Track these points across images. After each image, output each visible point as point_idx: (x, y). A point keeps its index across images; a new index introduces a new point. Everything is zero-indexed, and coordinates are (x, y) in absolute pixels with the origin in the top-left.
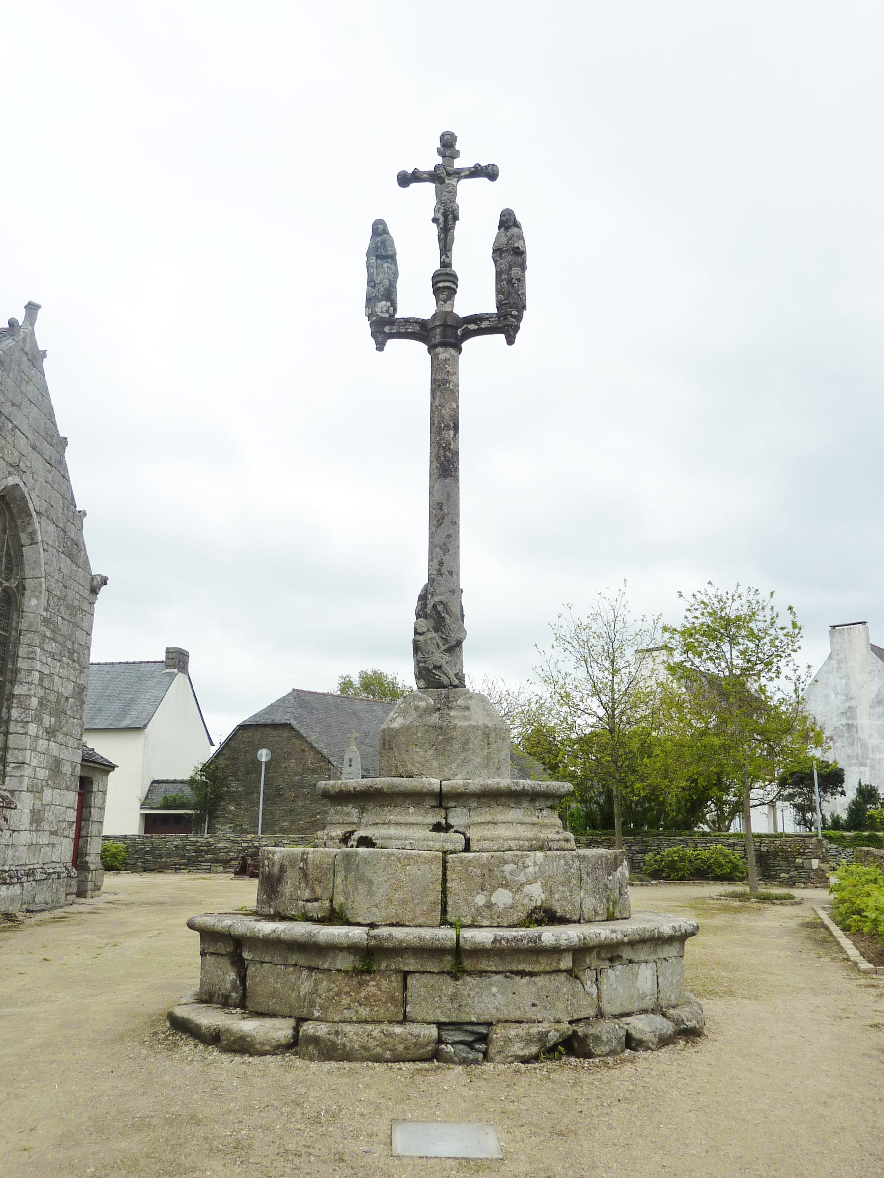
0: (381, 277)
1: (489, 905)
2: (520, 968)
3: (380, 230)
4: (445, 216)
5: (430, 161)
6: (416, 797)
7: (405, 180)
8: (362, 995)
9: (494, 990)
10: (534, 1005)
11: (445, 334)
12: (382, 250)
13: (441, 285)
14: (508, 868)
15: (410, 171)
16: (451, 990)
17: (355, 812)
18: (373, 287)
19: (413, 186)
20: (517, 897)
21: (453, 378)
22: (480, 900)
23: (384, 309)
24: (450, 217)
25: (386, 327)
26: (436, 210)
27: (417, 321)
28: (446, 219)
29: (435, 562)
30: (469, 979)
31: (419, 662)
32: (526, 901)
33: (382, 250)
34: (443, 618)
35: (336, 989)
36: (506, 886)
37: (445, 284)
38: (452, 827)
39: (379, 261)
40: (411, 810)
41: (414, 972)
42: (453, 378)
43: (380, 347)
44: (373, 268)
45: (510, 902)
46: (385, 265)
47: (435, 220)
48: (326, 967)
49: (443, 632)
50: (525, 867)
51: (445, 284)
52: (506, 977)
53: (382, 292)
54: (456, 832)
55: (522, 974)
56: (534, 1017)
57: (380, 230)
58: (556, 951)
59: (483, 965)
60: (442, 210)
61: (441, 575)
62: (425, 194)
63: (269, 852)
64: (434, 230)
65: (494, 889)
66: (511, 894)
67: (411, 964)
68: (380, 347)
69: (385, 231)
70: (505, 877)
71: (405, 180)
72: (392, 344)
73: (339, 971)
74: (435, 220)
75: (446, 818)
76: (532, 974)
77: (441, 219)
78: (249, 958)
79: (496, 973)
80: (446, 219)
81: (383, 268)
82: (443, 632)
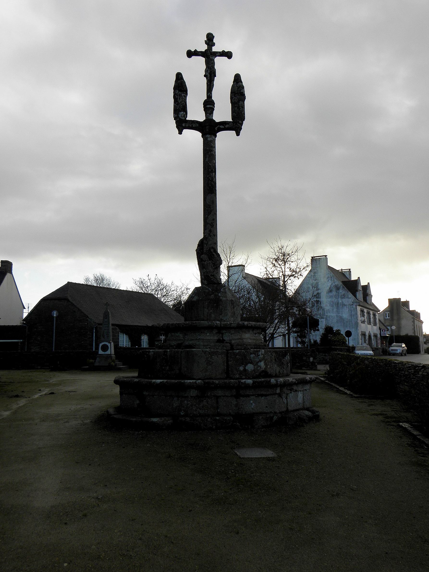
0: (181, 100)
1: (245, 370)
2: (262, 393)
3: (179, 77)
4: (210, 74)
5: (203, 48)
6: (210, 328)
7: (190, 54)
8: (201, 406)
9: (252, 402)
10: (267, 407)
11: (209, 129)
12: (180, 88)
13: (208, 106)
14: (252, 356)
15: (193, 50)
16: (235, 403)
17: (181, 336)
18: (178, 104)
19: (193, 57)
20: (255, 367)
21: (214, 149)
22: (241, 368)
23: (183, 115)
24: (213, 75)
25: (182, 123)
26: (206, 71)
27: (197, 122)
28: (211, 74)
29: (207, 231)
30: (242, 398)
31: (204, 273)
32: (259, 368)
33: (180, 88)
34: (213, 255)
35: (191, 404)
36: (251, 363)
37: (209, 105)
38: (225, 340)
39: (180, 93)
40: (208, 334)
41: (221, 396)
42: (214, 149)
43: (180, 133)
44: (177, 96)
45: (253, 369)
46: (183, 95)
47: (205, 76)
48: (186, 395)
49: (213, 261)
50: (258, 356)
51: (209, 105)
52: (256, 397)
53: (180, 108)
54: (226, 343)
55: (262, 395)
56: (266, 411)
57: (179, 77)
58: (276, 386)
59: (248, 393)
60: (209, 71)
61: (210, 236)
62: (200, 62)
63: (147, 352)
64: (205, 80)
65: (246, 364)
66: (253, 366)
67: (220, 393)
68: (180, 133)
69: (182, 78)
70: (251, 360)
71: (190, 54)
72: (185, 131)
73: (192, 397)
74: (205, 76)
75: (222, 337)
76: (266, 395)
77: (209, 76)
78: (147, 394)
79: (252, 395)
80: (211, 74)
81: (182, 96)
82: (213, 261)
